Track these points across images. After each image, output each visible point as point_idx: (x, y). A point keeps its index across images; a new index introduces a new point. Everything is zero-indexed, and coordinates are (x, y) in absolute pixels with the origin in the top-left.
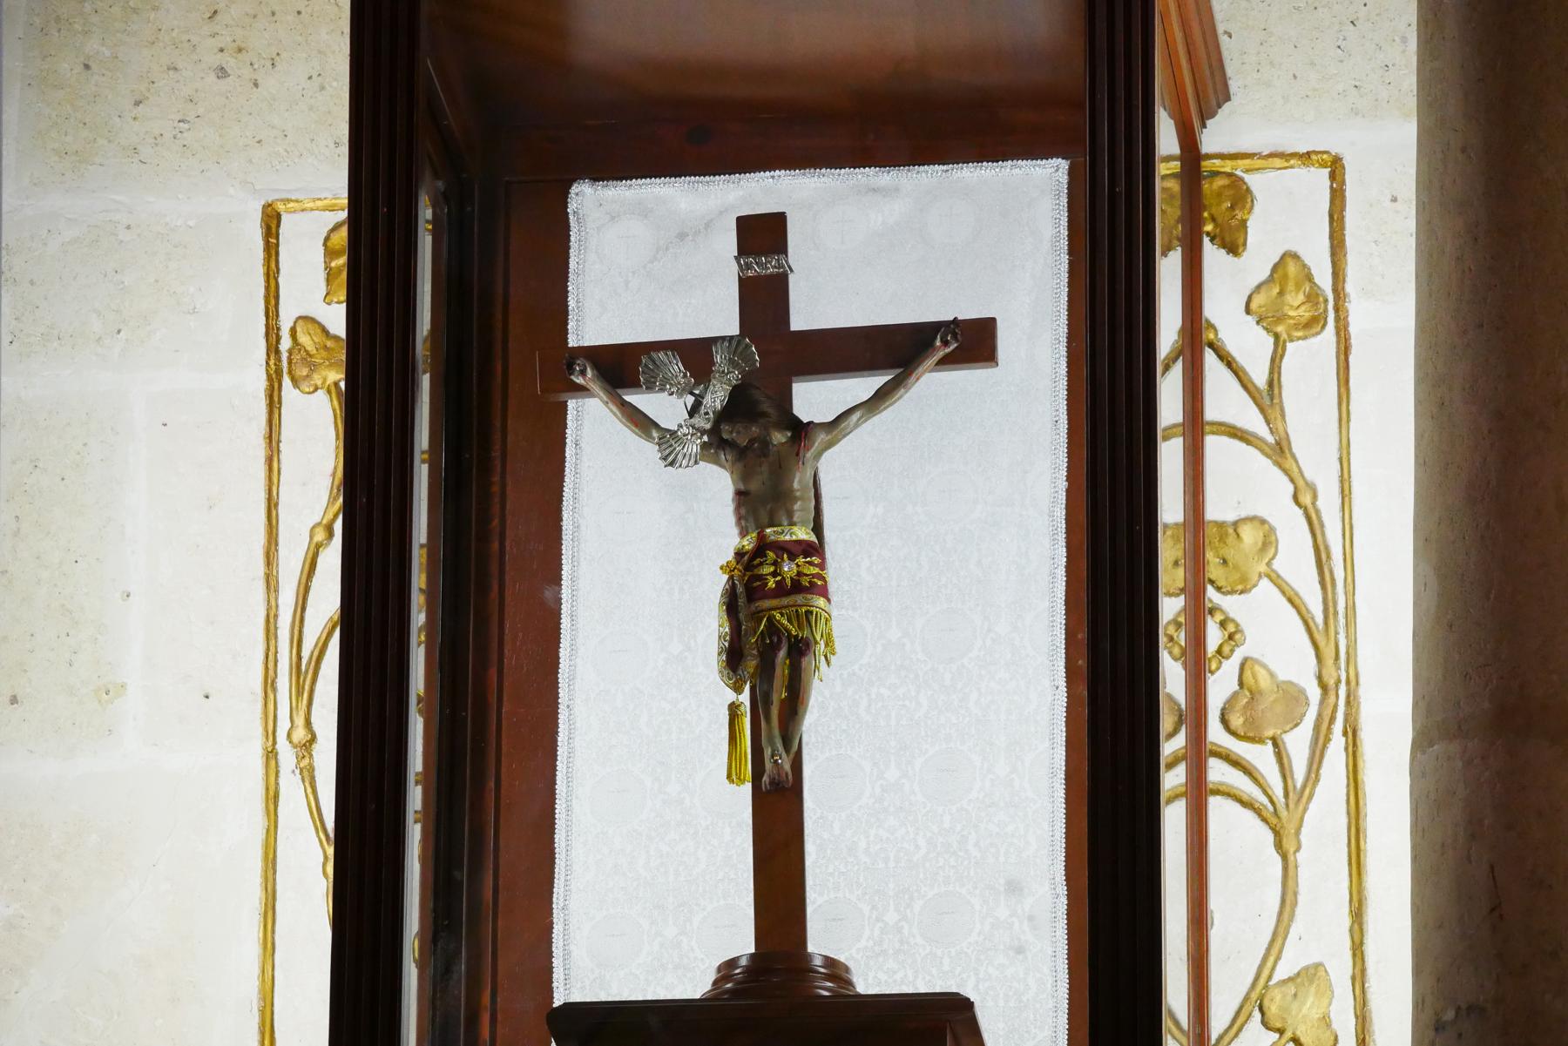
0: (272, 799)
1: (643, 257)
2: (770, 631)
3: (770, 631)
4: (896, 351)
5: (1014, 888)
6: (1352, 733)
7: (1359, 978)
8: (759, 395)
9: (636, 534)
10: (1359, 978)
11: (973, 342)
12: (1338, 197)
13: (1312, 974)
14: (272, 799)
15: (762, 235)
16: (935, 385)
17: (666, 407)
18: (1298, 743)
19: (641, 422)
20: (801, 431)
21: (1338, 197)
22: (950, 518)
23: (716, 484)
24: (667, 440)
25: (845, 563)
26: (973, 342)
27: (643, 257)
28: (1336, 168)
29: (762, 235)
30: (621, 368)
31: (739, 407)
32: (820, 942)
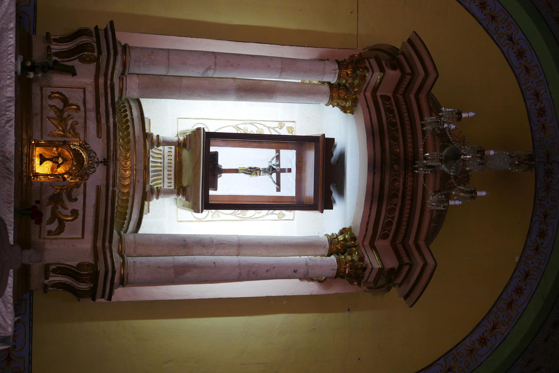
0: (240, 120)
1: (288, 157)
2: (252, 171)
3: (252, 171)
4: (278, 183)
5: (228, 190)
6: (241, 220)
7: (218, 221)
8: (275, 170)
9: (262, 157)
10: (218, 221)
11: (278, 190)
12: (290, 220)
13: (219, 216)
14: (240, 120)
15: (290, 170)
16: (275, 186)
17: (274, 162)
18: (240, 215)
19: (273, 159)
20: (271, 174)
21: (290, 220)
22: (263, 187)
23: (267, 166)
24: (271, 162)
25: (259, 177)
26: (278, 190)
27: (288, 157)
28: (293, 220)
29: (290, 170)
30: (278, 157)
31: (273, 169)
32: (223, 175)
